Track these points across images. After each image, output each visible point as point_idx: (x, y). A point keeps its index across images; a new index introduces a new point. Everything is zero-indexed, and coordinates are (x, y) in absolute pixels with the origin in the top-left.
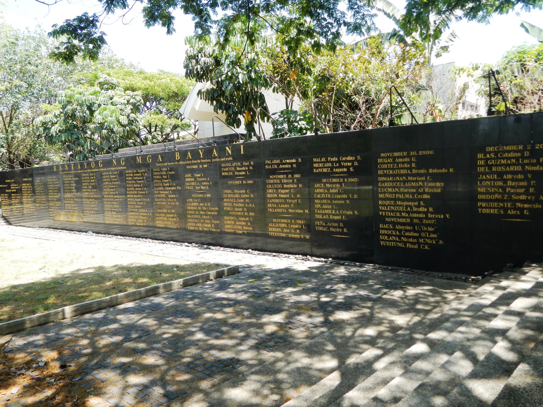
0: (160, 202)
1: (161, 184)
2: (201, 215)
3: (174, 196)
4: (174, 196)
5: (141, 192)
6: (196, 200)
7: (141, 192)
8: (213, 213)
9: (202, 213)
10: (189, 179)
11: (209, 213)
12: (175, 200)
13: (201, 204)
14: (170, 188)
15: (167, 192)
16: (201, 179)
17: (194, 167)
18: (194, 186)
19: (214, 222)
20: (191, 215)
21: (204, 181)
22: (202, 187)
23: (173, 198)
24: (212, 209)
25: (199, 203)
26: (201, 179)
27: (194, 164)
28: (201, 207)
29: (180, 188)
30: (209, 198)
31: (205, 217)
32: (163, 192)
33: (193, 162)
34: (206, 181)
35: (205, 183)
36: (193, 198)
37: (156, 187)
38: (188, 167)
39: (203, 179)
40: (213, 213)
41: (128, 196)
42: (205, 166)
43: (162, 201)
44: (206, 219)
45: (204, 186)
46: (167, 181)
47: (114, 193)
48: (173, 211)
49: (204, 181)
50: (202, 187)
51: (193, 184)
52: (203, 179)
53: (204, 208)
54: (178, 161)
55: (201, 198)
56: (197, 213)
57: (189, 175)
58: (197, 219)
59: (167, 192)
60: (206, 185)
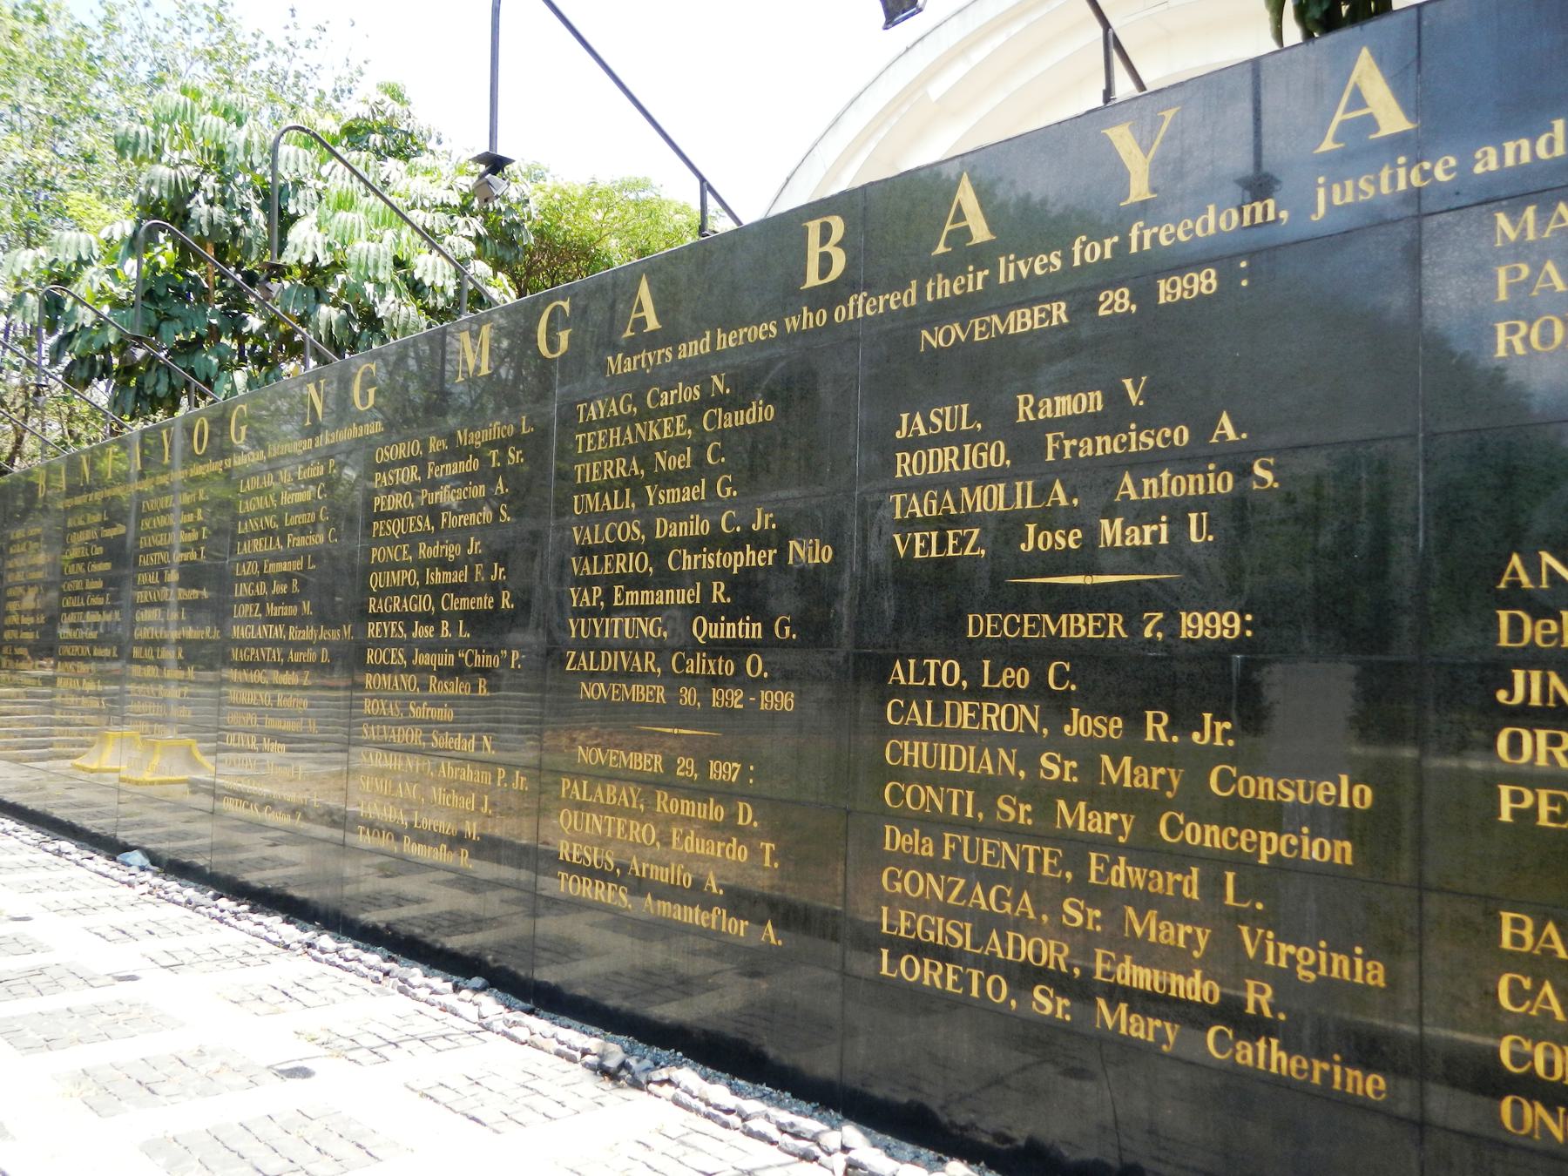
0: (612, 676)
1: (634, 530)
2: (1076, 847)
3: (755, 631)
4: (755, 631)
5: (465, 603)
6: (1020, 677)
7: (465, 603)
8: (1271, 845)
9: (1097, 823)
10: (945, 460)
11: (1213, 837)
12: (755, 665)
13: (1079, 725)
14: (710, 561)
15: (683, 597)
16: (1107, 445)
17: (1024, 321)
18: (1008, 527)
19: (1279, 953)
20: (933, 824)
21: (1146, 464)
22: (1111, 532)
23: (736, 649)
24: (1261, 788)
25: (1056, 707)
26: (1107, 445)
27: (1026, 293)
28: (1086, 753)
29: (825, 555)
30: (1218, 651)
31: (1123, 874)
32: (647, 597)
33: (1009, 270)
34: (1185, 461)
35: (1164, 485)
36: (969, 654)
37: (586, 551)
38: (934, 339)
39: (1141, 440)
40: (1271, 845)
41: (373, 630)
42: (1205, 282)
43: (630, 676)
44: (1144, 900)
45: (1142, 513)
46: (689, 494)
47: (290, 611)
48: (725, 771)
49: (1146, 464)
50: (1111, 532)
51: (990, 499)
52: (1141, 440)
53: (1123, 772)
54: (830, 296)
55: (1083, 654)
56: (1019, 813)
57: (951, 415)
58: (1018, 880)
59: (683, 597)
60: (1176, 511)
